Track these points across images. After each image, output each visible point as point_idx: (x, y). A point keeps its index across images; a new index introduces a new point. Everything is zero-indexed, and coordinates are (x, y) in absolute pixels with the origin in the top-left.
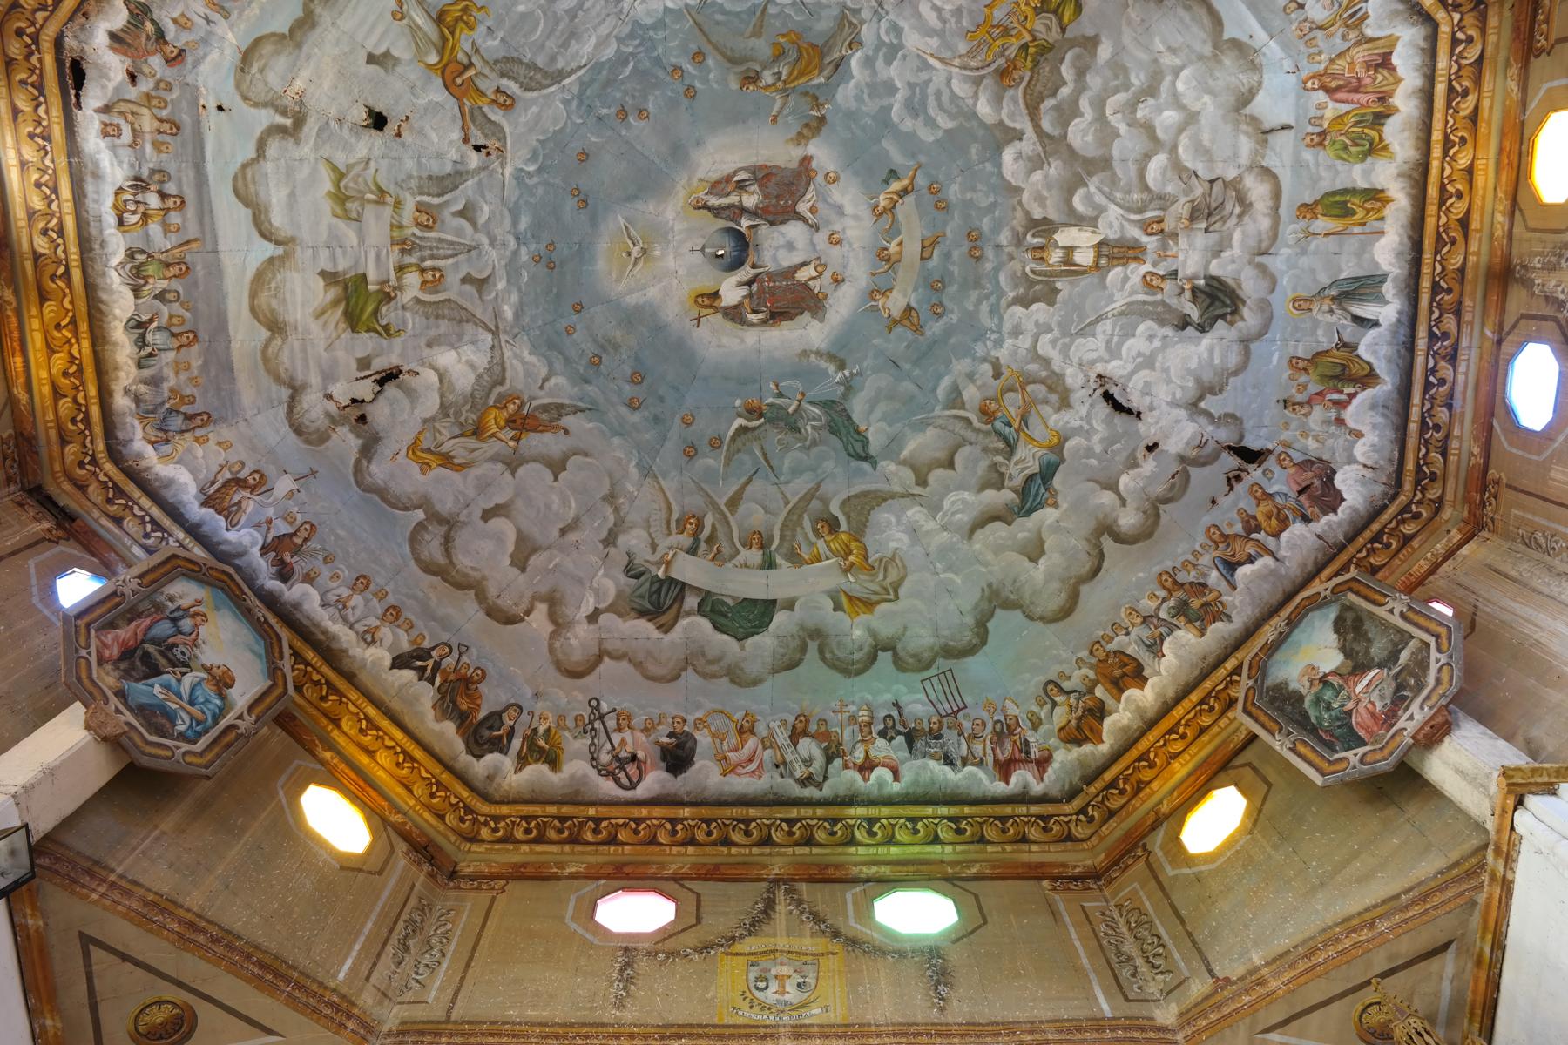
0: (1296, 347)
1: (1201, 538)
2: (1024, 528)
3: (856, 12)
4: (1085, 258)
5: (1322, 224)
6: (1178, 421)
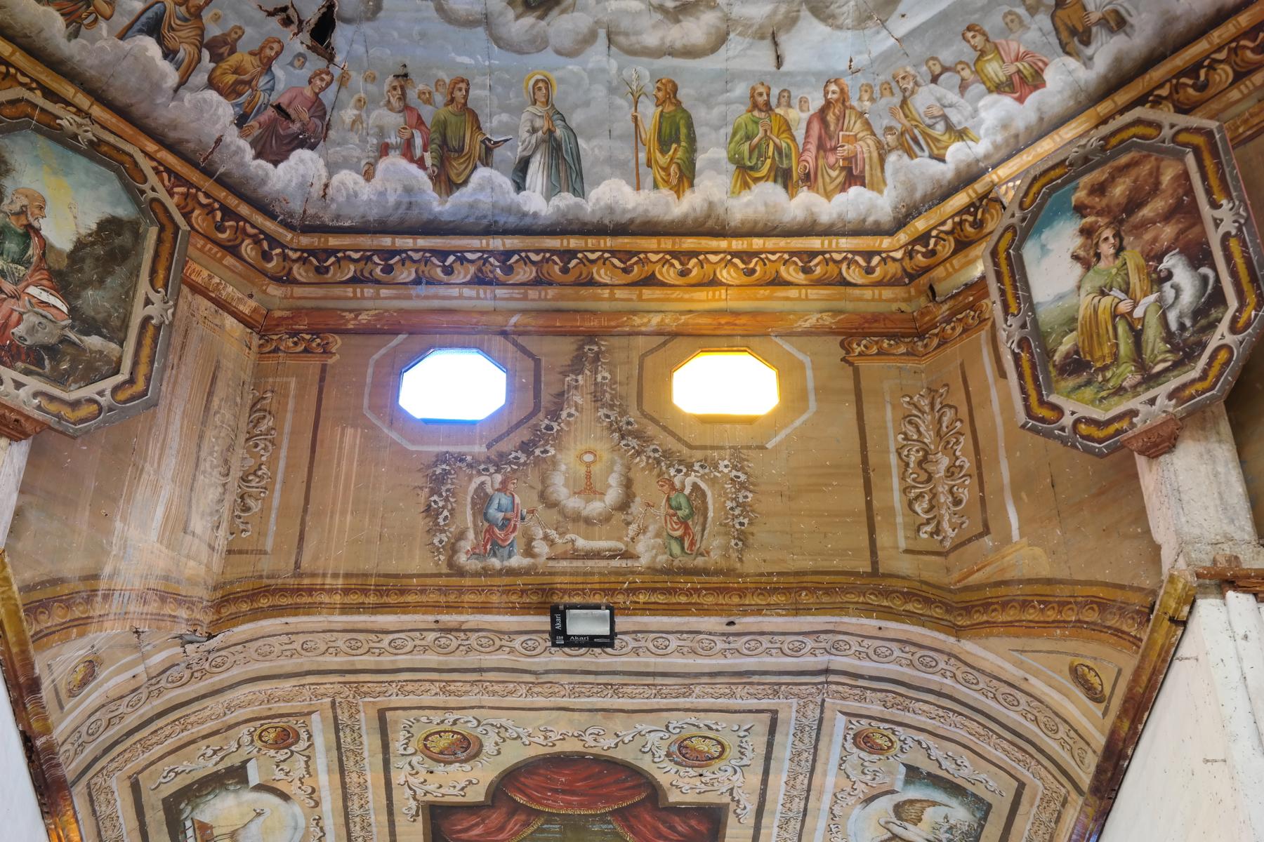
0: (483, 87)
5: (650, 112)
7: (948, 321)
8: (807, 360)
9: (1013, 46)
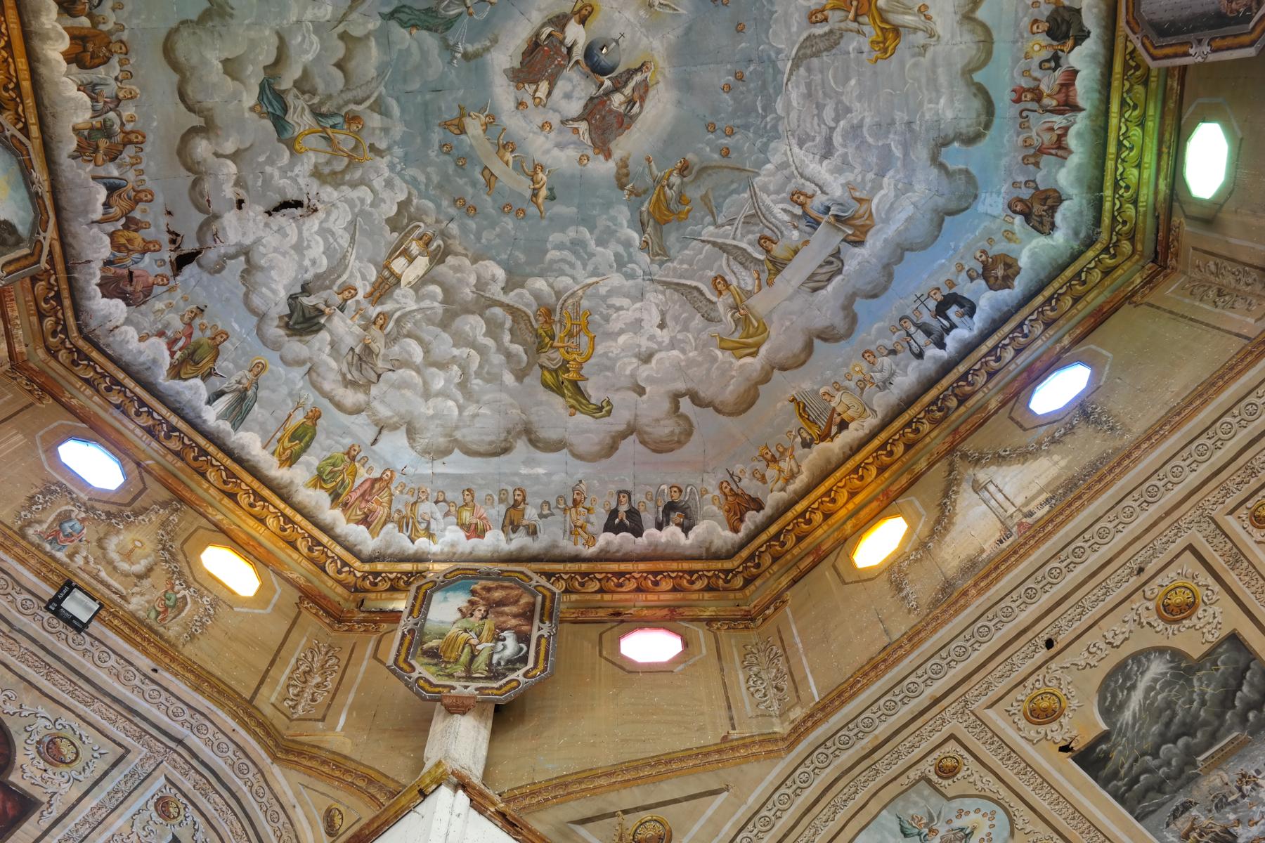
0: (233, 344)
1: (149, 184)
2: (254, 75)
3: (661, 264)
4: (399, 264)
5: (299, 417)
6: (244, 234)
7: (358, 623)
8: (279, 591)
9: (482, 511)
